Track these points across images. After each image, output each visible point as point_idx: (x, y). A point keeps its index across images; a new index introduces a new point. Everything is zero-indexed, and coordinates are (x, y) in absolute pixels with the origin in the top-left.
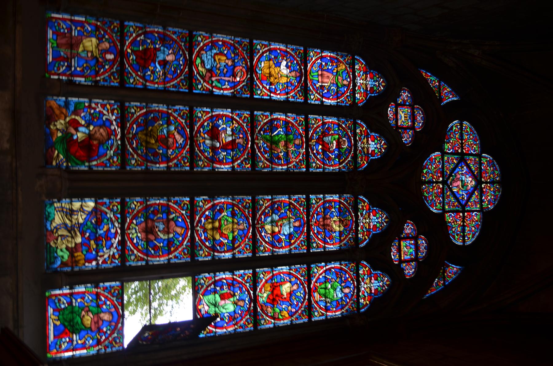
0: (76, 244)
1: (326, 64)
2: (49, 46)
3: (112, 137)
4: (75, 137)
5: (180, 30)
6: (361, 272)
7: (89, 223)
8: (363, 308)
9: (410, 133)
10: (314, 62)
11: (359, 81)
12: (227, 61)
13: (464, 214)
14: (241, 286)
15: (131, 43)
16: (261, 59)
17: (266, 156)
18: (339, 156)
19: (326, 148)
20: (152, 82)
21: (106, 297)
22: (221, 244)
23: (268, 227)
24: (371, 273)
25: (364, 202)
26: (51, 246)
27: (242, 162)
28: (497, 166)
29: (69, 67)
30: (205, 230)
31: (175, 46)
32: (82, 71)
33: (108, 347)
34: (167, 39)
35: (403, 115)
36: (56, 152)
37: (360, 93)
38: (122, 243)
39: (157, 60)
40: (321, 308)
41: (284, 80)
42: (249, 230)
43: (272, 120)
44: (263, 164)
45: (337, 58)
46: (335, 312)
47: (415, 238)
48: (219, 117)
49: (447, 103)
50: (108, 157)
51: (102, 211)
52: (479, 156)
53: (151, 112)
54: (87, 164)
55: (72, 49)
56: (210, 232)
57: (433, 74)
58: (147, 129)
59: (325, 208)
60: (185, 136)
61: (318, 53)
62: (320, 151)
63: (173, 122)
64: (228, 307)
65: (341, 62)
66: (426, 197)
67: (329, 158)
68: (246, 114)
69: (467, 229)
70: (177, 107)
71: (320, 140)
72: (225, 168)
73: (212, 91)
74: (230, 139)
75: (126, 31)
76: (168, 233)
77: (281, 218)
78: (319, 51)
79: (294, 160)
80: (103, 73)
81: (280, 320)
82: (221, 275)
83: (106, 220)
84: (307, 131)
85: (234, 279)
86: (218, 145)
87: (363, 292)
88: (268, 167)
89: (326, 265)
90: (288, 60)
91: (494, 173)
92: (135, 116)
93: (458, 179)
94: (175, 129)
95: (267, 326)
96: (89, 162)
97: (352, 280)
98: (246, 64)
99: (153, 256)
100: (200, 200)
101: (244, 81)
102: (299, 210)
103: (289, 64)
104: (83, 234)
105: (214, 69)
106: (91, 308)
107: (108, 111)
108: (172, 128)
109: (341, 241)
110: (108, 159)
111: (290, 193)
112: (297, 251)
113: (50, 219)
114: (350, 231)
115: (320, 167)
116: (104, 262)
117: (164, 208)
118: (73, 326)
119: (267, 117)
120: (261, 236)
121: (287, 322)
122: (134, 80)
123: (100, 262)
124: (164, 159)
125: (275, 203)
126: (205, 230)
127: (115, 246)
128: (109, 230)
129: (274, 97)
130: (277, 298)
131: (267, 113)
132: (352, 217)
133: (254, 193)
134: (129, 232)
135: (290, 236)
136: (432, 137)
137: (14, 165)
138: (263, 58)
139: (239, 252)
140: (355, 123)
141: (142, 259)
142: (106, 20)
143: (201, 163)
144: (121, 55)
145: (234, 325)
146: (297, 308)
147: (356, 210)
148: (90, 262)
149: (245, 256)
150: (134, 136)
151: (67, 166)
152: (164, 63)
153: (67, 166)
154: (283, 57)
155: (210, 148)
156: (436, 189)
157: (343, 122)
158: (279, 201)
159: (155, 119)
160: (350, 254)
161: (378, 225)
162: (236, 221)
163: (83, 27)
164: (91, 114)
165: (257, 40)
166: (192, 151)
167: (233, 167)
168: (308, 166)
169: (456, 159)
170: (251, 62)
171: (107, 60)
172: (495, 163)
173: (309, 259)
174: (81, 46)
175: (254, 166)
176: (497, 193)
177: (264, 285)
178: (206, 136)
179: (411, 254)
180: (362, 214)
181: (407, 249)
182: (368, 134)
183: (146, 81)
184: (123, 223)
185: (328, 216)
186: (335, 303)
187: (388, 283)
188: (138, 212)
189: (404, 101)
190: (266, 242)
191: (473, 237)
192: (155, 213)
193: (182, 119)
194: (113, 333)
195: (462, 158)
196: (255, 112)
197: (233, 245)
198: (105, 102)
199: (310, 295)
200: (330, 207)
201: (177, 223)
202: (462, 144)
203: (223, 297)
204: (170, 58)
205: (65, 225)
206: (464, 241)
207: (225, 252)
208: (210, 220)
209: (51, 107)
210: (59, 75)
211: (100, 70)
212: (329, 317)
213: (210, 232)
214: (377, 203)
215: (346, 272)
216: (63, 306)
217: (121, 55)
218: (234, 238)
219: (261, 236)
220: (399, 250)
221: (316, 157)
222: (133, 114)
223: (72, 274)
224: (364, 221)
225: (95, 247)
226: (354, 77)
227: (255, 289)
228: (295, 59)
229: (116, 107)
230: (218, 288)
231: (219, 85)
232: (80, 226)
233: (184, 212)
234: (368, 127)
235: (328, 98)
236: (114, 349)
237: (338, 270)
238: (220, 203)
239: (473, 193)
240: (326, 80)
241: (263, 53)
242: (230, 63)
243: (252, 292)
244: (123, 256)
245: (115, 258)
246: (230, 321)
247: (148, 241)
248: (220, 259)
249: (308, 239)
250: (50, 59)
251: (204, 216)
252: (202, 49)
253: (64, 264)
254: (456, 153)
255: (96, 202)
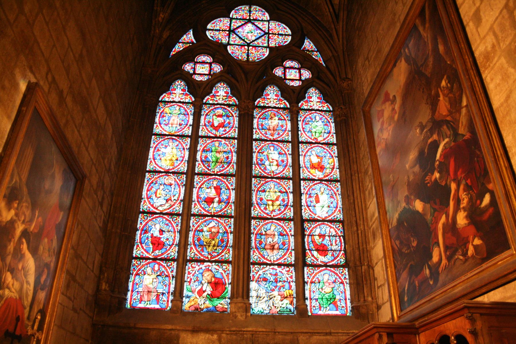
0: (279, 295)
1: (165, 121)
2: (149, 306)
3: (210, 268)
4: (210, 293)
5: (139, 219)
6: (306, 107)
7: (266, 286)
8: (329, 108)
9: (213, 65)
10: (163, 129)
11: (177, 100)
12: (161, 189)
13: (271, 34)
14: (311, 189)
15: (147, 252)
16: (160, 166)
17: (226, 166)
18: (228, 116)
19: (222, 125)
20: (174, 240)
21: (314, 277)
22: (283, 200)
23: (274, 168)
24: (307, 101)
25: (259, 101)
26: (280, 311)
27: (229, 183)
28: (239, 7)
29: (163, 294)
30: (274, 211)
31: (150, 223)
32: (166, 286)
33: (345, 277)
34: (145, 228)
35: (201, 70)
36: (219, 305)
37: (186, 98)
38: (279, 265)
39: (159, 236)
40: (328, 136)
41: (175, 151)
42: (274, 181)
43: (202, 161)
44: (232, 170)
45: (161, 113)
46: (331, 127)
47: (285, 68)
48: (198, 197)
49: (195, 38)
50: (223, 272)
51: (258, 278)
52: (231, 19)
53: (194, 242)
54: (227, 285)
55: (151, 292)
56: (275, 207)
57: (174, 46)
58: (205, 245)
59: (263, 129)
60: (211, 221)
61: (157, 126)
62: (223, 129)
63: (201, 228)
64: (324, 199)
65: (163, 110)
66: (258, 59)
67: (229, 123)
68: (196, 178)
69: (280, 32)
70: (191, 225)
71: (216, 129)
72: (233, 194)
73: (181, 200)
74: (213, 191)
75: (139, 256)
76: (274, 235)
77: (268, 159)
78: (155, 125)
79: (229, 148)
80: (168, 272)
81: (334, 164)
82: (303, 202)
83: (264, 275)
84: (210, 137)
85: (307, 193)
86: (217, 199)
87: (319, 107)
88: (233, 166)
89: (300, 131)
90: (161, 147)
91: (243, 10)
92: (196, 253)
93: (247, 35)
94: (205, 226)
95: (338, 173)
96: (226, 284)
97: (311, 114)
98: (163, 176)
99: (289, 246)
100: (254, 213)
101: (175, 179)
102: (263, 146)
103: (164, 146)
104: (273, 290)
105: (166, 198)
106: (320, 287)
107: (193, 271)
108: (205, 229)
109: (285, 119)
110: (225, 273)
111: (251, 152)
112: (290, 150)
113: (262, 311)
114: (278, 113)
115: (235, 130)
116: (291, 277)
117: (258, 237)
118: (331, 299)
119: (199, 164)
120: (279, 173)
121: (336, 160)
122: (173, 253)
123: (291, 280)
124: (226, 235)
125: (257, 162)
126: (274, 211)
127: (281, 270)
128: (271, 274)
129: (186, 158)
130: (321, 165)
131: (197, 163)
132: (269, 111)
133: (250, 176)
134: (272, 261)
135: (280, 153)
136: (218, 52)
137: (227, 332)
138: (160, 164)
139: (289, 188)
140: (206, 104)
141: (291, 253)
142: (132, 268)
143: (229, 211)
144: (155, 259)
145: (336, 195)
146: (328, 152)
147: (264, 108)
148: (290, 287)
149: (291, 185)
150: (209, 254)
151: (229, 298)
152: (161, 231)
153: (228, 298)
154: (158, 150)
155: (219, 204)
156: (252, 50)
157: (205, 112)
158: (256, 160)
159: (199, 240)
160: (294, 113)
161: (275, 93)
162: (268, 190)
163: (137, 284)
164: (195, 282)
165: (146, 168)
166: (220, 216)
167: (232, 189)
168: (234, 138)
169: (233, 35)
170: (162, 172)
171: (159, 269)
172: (237, 8)
173: (296, 143)
174: (149, 286)
175: (232, 175)
176: (257, 9)
177: (311, 174)
178: (211, 206)
179: (296, 72)
180: (267, 104)
181: (292, 74)
182: (213, 95)
183: (173, 244)
184: (267, 264)
185: (268, 127)
186: (326, 127)
187: (314, 90)
188: (260, 254)
189: (192, 68)
190: (283, 170)
191: (286, 29)
192: (261, 243)
193: (199, 221)
194: (336, 274)
195: (231, 31)
196: (196, 172)
197: (284, 192)
198: (187, 272)
199: (319, 143)
200: (262, 125)
201: (268, 229)
202: (223, 30)
203: (318, 201)
204: (158, 227)
205: (266, 302)
206: (289, 35)
207: (288, 198)
208: (267, 207)
209: (189, 308)
210: (168, 301)
211: (165, 274)
212: (334, 132)
213: (275, 207)
214: (260, 93)
215: (305, 117)
216: (318, 304)
217: (155, 259)
218: (280, 192)
219: (279, 173)
220: (292, 80)
221: (228, 132)
222: (195, 254)
223: (297, 298)
224: (272, 102)
225: (281, 283)
226: (174, 102)
227: (314, 180)
228: (160, 142)
229: (190, 265)
230: (312, 204)
231: (177, 196)
232: (267, 292)
233: (261, 224)
234: (208, 94)
235: (188, 121)
236: (347, 273)
237: (304, 123)
238: (256, 199)
239: (256, 26)
240: (175, 122)
241: (156, 164)
242: (162, 187)
243: (316, 182)
244: (288, 265)
245: (289, 270)
246: (333, 198)
247: (279, 249)
248: (293, 202)
249: (282, 141)
250: (157, 307)
251: (264, 211)
252: (152, 206)
253: (291, 303)
254: (229, 35)
255: (253, 281)
